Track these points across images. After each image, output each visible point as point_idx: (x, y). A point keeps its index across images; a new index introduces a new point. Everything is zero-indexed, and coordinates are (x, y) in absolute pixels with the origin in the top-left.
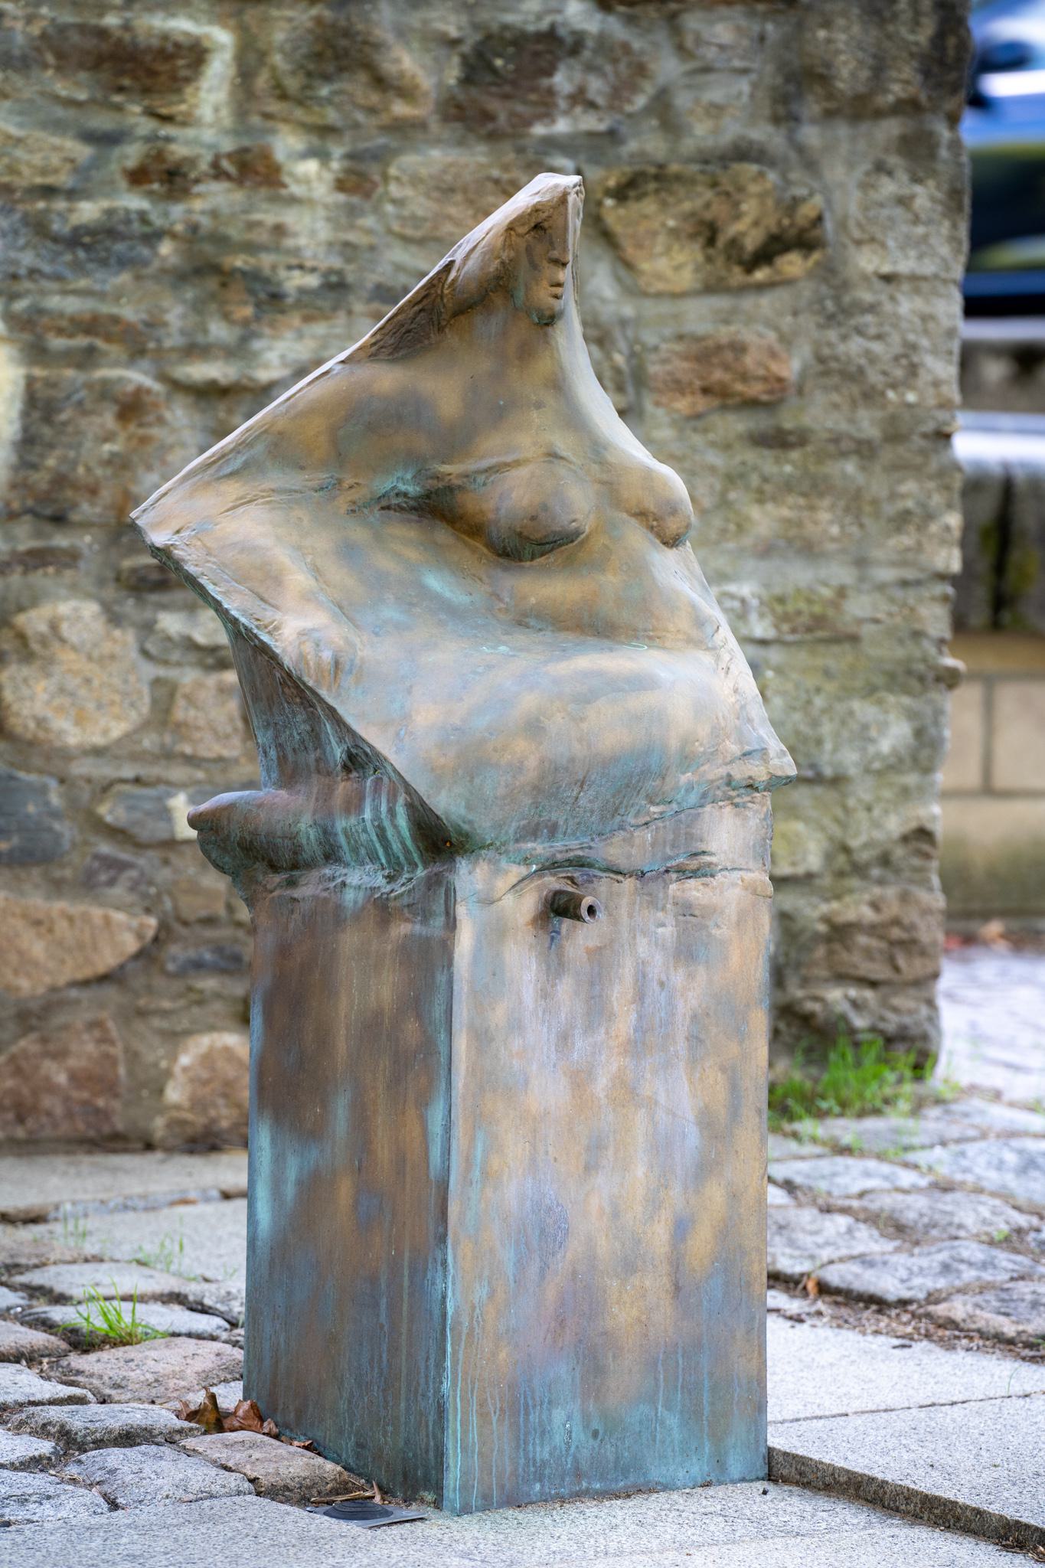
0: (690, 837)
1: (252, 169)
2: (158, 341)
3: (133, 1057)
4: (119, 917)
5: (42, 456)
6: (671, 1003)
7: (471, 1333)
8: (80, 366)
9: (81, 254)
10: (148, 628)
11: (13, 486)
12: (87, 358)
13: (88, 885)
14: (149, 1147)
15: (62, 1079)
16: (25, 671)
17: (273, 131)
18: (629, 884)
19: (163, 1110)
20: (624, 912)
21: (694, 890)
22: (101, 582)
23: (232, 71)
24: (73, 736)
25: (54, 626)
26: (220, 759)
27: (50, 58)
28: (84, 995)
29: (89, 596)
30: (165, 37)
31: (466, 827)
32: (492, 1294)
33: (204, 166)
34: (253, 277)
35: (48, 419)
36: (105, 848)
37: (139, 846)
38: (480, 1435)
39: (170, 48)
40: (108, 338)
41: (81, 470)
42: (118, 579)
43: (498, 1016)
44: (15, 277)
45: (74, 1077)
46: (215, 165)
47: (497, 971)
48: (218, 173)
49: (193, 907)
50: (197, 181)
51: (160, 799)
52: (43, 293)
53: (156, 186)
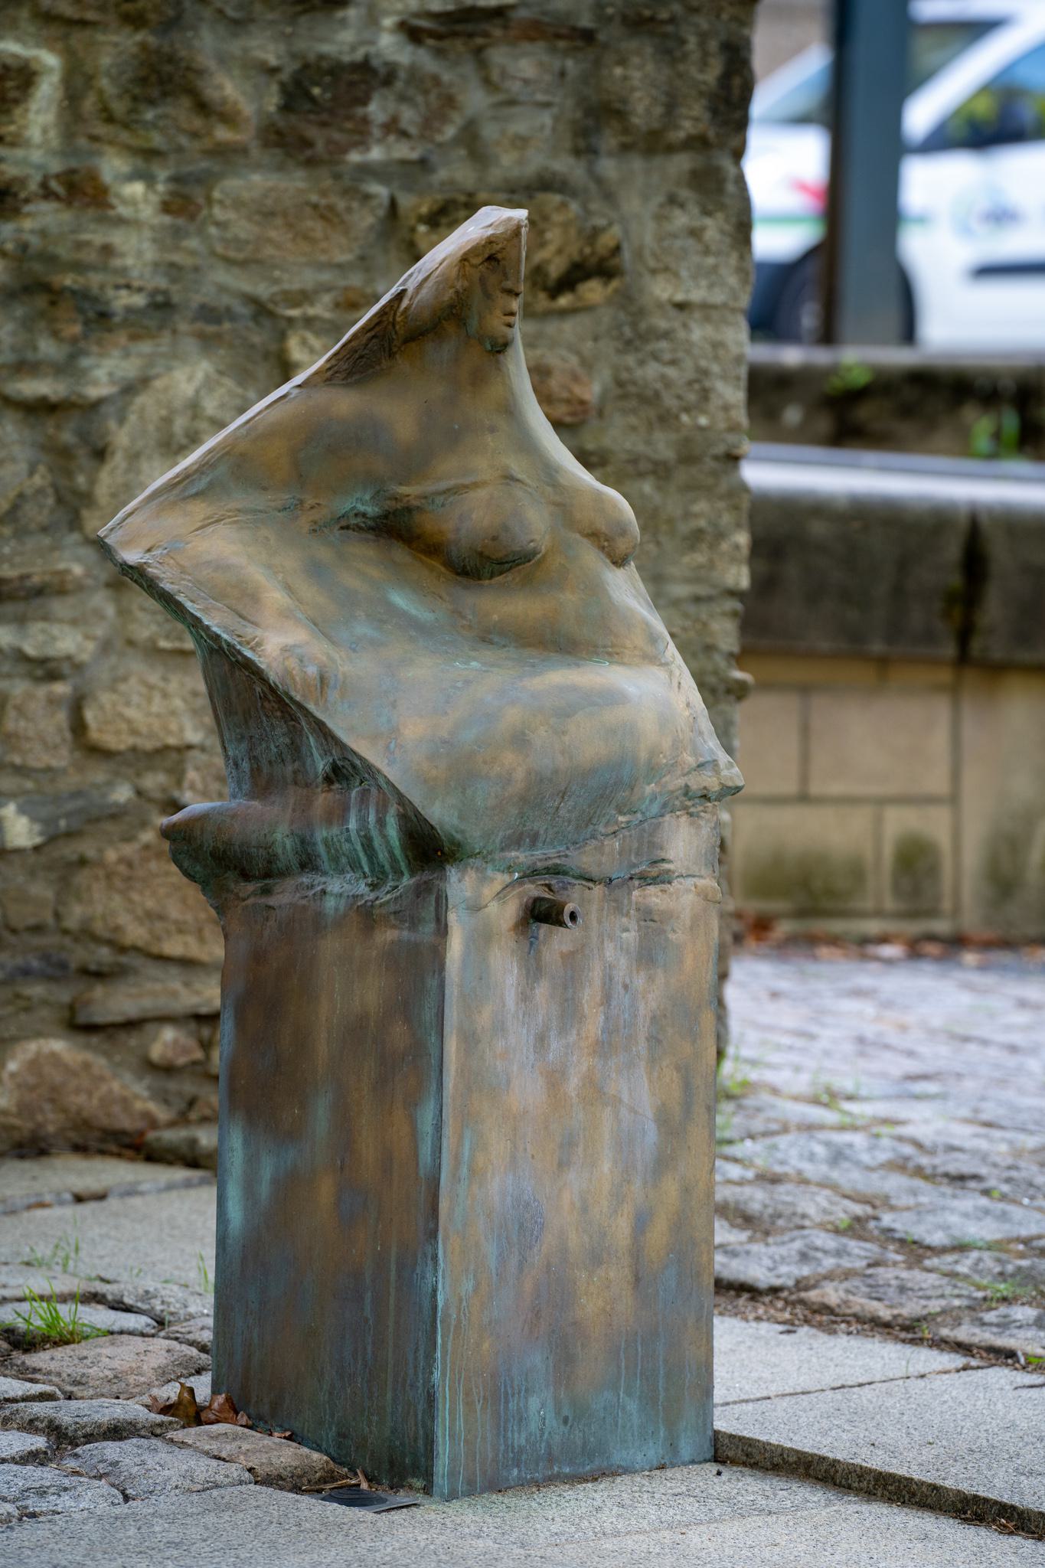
1: (80, 190)
17: (100, 154)
21: (653, 897)
23: (59, 94)
26: (49, 769)
46: (44, 185)
48: (48, 194)
50: (27, 201)
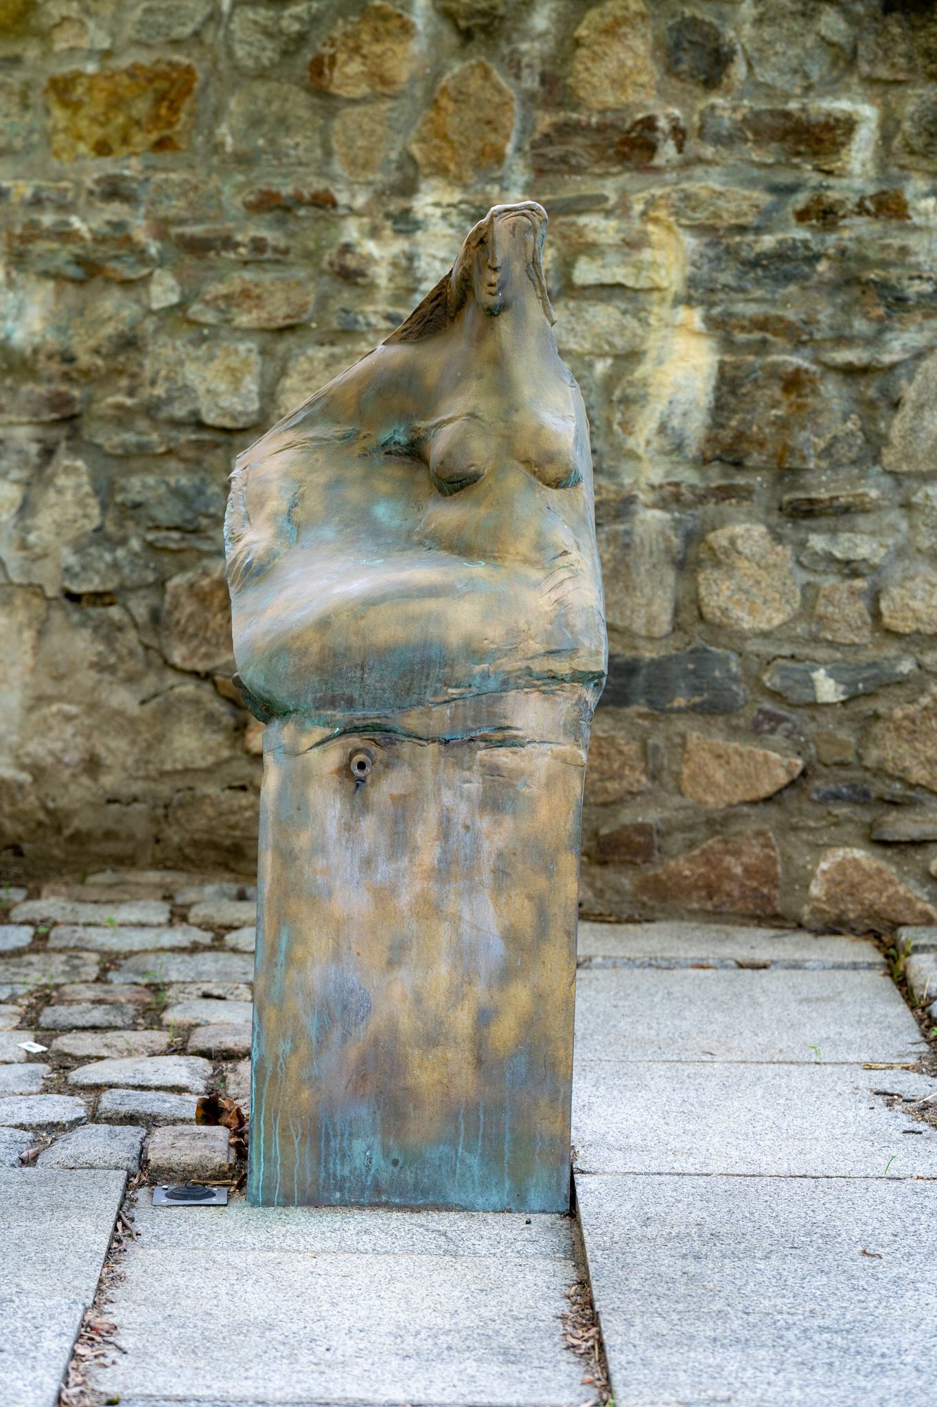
0: (492, 715)
1: (888, 206)
2: (811, 334)
3: (788, 860)
4: (775, 756)
5: (729, 419)
6: (476, 842)
7: (274, 1076)
8: (757, 354)
9: (760, 272)
10: (802, 545)
11: (708, 440)
12: (763, 347)
13: (756, 731)
14: (800, 926)
15: (738, 870)
16: (716, 574)
17: (907, 178)
18: (432, 748)
19: (809, 900)
20: (428, 769)
21: (503, 757)
22: (768, 511)
23: (877, 135)
24: (747, 623)
25: (732, 541)
26: (853, 645)
27: (750, 135)
28: (753, 811)
29: (759, 521)
30: (829, 115)
31: (266, 696)
32: (295, 1049)
33: (850, 206)
34: (883, 287)
35: (733, 392)
36: (768, 705)
37: (794, 706)
38: (282, 1151)
39: (832, 121)
40: (775, 334)
41: (755, 428)
42: (780, 509)
43: (303, 840)
44: (712, 291)
45: (746, 870)
46: (860, 205)
47: (302, 807)
48: (861, 210)
49: (831, 753)
50: (844, 217)
51: (806, 672)
52: (732, 301)
53: (814, 222)
